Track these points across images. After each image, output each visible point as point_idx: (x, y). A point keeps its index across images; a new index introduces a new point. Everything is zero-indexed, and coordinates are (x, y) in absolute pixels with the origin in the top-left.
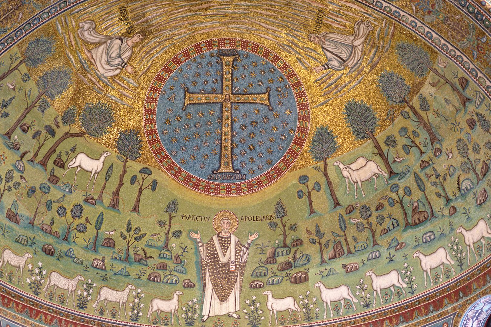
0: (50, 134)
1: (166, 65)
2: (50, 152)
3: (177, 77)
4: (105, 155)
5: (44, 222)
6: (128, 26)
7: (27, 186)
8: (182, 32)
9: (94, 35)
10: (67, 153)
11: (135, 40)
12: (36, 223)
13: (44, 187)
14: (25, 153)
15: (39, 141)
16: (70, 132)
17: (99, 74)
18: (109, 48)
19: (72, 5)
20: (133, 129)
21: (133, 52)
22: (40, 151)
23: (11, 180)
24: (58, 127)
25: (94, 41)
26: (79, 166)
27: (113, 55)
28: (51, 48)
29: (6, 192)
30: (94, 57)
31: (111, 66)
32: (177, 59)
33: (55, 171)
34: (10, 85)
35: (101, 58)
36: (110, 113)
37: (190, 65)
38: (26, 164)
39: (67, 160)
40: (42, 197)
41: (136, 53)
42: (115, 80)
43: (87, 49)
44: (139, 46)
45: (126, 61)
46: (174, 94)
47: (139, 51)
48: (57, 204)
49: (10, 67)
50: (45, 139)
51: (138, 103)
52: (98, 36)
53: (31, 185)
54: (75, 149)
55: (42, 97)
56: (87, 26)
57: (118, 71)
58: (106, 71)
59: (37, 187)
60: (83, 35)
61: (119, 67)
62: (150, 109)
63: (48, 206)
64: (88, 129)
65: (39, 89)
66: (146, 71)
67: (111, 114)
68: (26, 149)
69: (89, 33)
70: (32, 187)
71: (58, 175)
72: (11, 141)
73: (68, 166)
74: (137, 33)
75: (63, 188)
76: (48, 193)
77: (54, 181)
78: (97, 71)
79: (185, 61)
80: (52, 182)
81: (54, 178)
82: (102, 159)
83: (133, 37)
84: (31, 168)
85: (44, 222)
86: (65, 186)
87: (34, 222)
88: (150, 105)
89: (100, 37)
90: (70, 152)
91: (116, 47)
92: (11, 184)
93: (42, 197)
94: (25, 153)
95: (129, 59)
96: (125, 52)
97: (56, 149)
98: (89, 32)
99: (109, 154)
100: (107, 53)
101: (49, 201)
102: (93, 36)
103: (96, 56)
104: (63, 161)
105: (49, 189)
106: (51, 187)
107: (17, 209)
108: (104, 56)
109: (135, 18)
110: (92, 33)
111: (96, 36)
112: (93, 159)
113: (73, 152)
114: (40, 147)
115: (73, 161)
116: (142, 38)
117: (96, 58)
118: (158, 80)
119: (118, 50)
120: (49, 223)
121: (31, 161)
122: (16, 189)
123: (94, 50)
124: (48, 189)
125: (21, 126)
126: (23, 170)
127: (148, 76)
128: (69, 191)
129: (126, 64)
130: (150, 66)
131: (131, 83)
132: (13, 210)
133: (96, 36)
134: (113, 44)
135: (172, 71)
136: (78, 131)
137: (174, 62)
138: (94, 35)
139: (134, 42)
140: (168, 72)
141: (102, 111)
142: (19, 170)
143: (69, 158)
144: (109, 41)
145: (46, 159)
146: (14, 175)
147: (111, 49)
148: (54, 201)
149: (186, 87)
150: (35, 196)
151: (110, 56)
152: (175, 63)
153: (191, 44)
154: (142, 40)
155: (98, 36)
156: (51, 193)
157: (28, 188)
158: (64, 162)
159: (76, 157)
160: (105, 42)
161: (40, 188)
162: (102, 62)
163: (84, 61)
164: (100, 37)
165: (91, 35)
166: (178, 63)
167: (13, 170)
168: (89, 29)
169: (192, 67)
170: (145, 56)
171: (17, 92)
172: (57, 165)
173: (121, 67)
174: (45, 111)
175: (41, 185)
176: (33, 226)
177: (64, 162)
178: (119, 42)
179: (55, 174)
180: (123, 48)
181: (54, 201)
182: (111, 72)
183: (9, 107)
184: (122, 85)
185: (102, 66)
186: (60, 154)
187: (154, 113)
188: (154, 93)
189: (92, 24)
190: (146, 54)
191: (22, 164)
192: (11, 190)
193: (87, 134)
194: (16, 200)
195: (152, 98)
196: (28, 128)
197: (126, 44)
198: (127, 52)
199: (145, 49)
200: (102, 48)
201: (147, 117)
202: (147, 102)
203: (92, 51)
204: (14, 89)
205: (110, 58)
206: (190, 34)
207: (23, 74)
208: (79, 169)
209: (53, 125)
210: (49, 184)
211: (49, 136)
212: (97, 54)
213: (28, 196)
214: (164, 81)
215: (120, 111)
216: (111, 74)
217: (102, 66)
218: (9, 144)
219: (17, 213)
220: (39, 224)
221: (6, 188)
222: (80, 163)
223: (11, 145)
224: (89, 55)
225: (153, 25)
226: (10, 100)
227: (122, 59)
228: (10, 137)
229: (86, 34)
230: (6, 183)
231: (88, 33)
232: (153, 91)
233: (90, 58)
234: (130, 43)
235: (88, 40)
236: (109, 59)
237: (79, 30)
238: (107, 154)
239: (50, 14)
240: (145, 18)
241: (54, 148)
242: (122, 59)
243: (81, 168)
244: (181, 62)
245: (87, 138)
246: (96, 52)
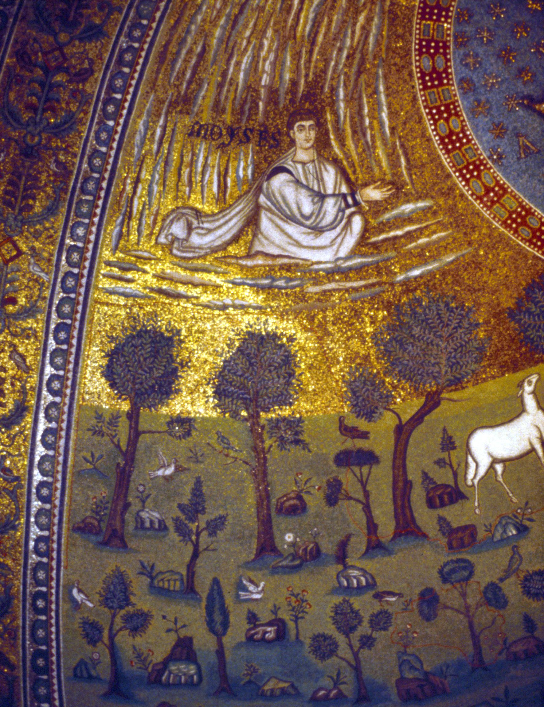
0: (360, 465)
1: (425, 107)
2: (398, 493)
3: (479, 101)
4: (528, 388)
5: (510, 641)
6: (255, 138)
7: (408, 603)
8: (363, 28)
9: (217, 224)
10: (440, 463)
11: (307, 141)
12: (489, 656)
13: (453, 571)
14: (343, 546)
15: (350, 498)
16: (404, 421)
17: (329, 266)
18: (280, 209)
19: (92, 237)
20: (528, 284)
21: (336, 162)
22: (376, 512)
23: (356, 622)
24: (365, 435)
25: (234, 231)
26: (495, 461)
27: (307, 208)
28: (162, 334)
29: (365, 653)
30: (276, 252)
31: (332, 226)
32: (430, 75)
33: (449, 518)
34: (160, 473)
35: (290, 237)
36: (442, 305)
37: (467, 55)
38: (370, 565)
39: (455, 474)
40: (464, 595)
41: (341, 156)
42: (373, 239)
43: (241, 258)
44: (329, 138)
45: (344, 189)
46: (518, 135)
47: (342, 145)
48: (513, 579)
49: (118, 446)
50: (361, 482)
51: (473, 228)
52: (227, 218)
53: (417, 591)
54: (450, 438)
55: (262, 422)
56: (178, 229)
57: (357, 223)
58: (335, 247)
59: (436, 583)
60: (192, 248)
61: (348, 212)
62: (511, 213)
63: (494, 602)
64: (435, 378)
65: (235, 415)
66: (408, 161)
67: (447, 305)
68: (338, 538)
69: (203, 232)
70: (422, 595)
71: (464, 521)
72: (286, 554)
73: (470, 483)
74: (290, 126)
75: (498, 536)
76: (471, 574)
77: (466, 540)
78: (316, 267)
79: (448, 60)
80: (462, 545)
81: (460, 535)
82: (530, 402)
83: (293, 142)
84: (386, 559)
85: (510, 641)
86: (500, 530)
87: (481, 660)
88: (503, 206)
89: (233, 213)
90: (445, 455)
91: (290, 192)
92: (364, 628)
93: (464, 595)
94: (343, 546)
95: (348, 181)
96: (320, 180)
97: (410, 477)
98: (200, 231)
99: (534, 379)
100: (291, 219)
101: (486, 588)
102: (220, 227)
103: (278, 246)
104: (448, 486)
105: (469, 567)
106: (469, 557)
107: (418, 666)
108: (291, 229)
109: (242, 112)
110: (206, 225)
111: (222, 221)
112: (511, 421)
113: (454, 448)
114: (367, 509)
115: (472, 465)
116: (311, 122)
117: (283, 249)
118: (455, 148)
119: (303, 191)
120: (521, 633)
121: (373, 548)
122: (385, 629)
123: (256, 243)
124: (464, 568)
125: (279, 511)
126: (370, 580)
127: (423, 165)
128: (517, 529)
129: (353, 195)
130: (402, 146)
131: (412, 212)
132: (409, 675)
133: (222, 221)
134: (277, 195)
135: (453, 103)
136: (417, 403)
137: (433, 86)
138: (217, 224)
139: (309, 145)
140: (450, 115)
141: (423, 317)
142: (360, 589)
143: (455, 466)
144: (262, 199)
145: (405, 515)
146: (356, 606)
147: (287, 205)
148: (502, 580)
149: (523, 98)
150: (446, 607)
151: (302, 215)
152: (437, 87)
153: (410, 21)
154: (320, 125)
155: (227, 218)
156: (478, 569)
157: (415, 606)
158: (452, 484)
159: (468, 451)
160: (257, 209)
161: (445, 577)
162: (305, 244)
163: (266, 278)
164: (233, 213)
165: (210, 231)
166: (440, 79)
167: (344, 600)
168: (190, 229)
169: (477, 55)
170: (367, 142)
171: (192, 465)
172: (443, 505)
173: (353, 209)
174: (301, 437)
175: (441, 572)
176: (485, 669)
177: (452, 484)
178: (282, 177)
179: (455, 525)
180: (307, 179)
181: (502, 580)
182: (348, 237)
183: (209, 505)
184: (399, 233)
185: (313, 248)
186: (425, 476)
187: (529, 212)
188: (479, 177)
189: (183, 214)
190: (364, 135)
191: (355, 573)
192: (375, 640)
193: (443, 388)
194: (402, 649)
195: (488, 190)
196: (299, 497)
197: (299, 166)
198: (325, 174)
199: (349, 131)
200: (265, 223)
201: (526, 232)
202: (489, 208)
203: (258, 247)
204: (179, 469)
205: (308, 218)
206: (382, 11)
207: (165, 428)
208: (499, 468)
209: (350, 444)
210: (459, 556)
211: (365, 469)
212: (273, 243)
213: (428, 619)
214: (466, 136)
215: (457, 281)
216: (350, 241)
217: (313, 248)
218: (284, 563)
219: (426, 674)
220: (500, 653)
221: (356, 644)
222: (490, 455)
223: (293, 560)
224: (260, 261)
225: (294, 83)
226: (197, 492)
227: (333, 195)
228: (274, 550)
229: (196, 240)
230: (347, 636)
231: (199, 234)
232: (472, 176)
233: (270, 262)
234: (302, 155)
235: (218, 243)
236: (308, 223)
237: (175, 251)
238: (530, 383)
239: (73, 296)
240: (262, 91)
241: (401, 478)
242: (333, 195)
243: (503, 461)
244: (445, 71)
245: (455, 395)
246: (265, 242)
